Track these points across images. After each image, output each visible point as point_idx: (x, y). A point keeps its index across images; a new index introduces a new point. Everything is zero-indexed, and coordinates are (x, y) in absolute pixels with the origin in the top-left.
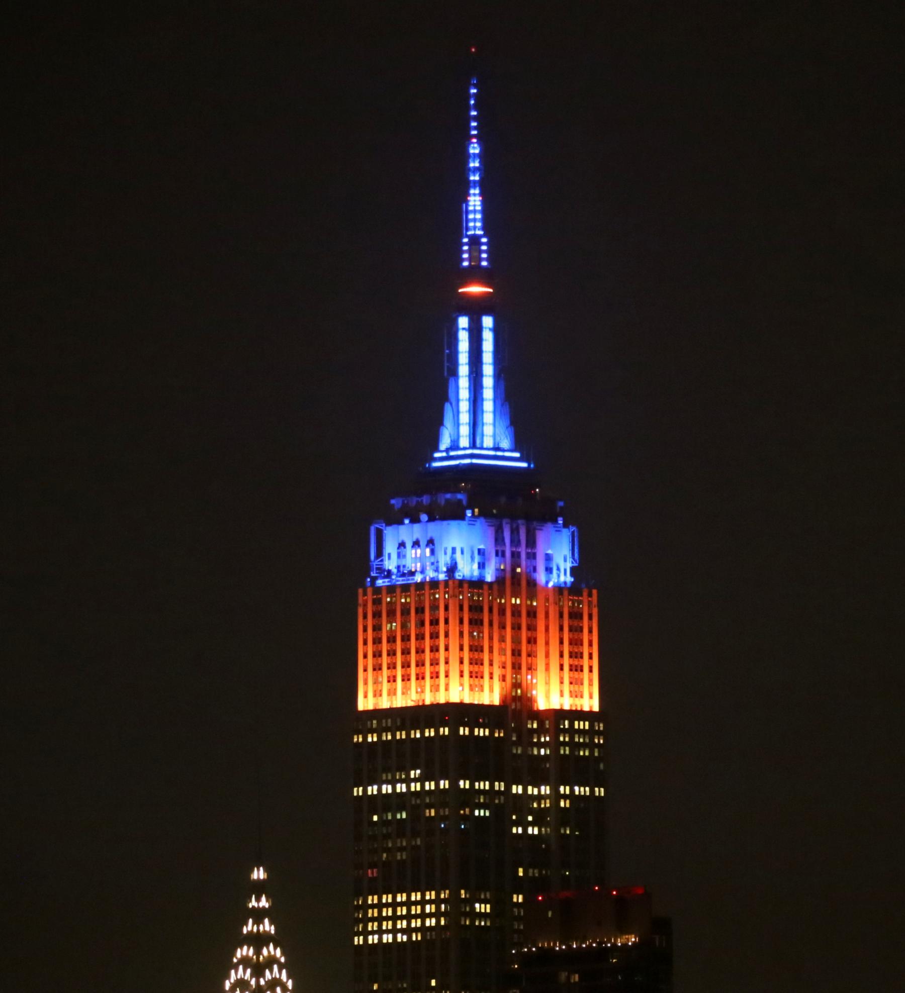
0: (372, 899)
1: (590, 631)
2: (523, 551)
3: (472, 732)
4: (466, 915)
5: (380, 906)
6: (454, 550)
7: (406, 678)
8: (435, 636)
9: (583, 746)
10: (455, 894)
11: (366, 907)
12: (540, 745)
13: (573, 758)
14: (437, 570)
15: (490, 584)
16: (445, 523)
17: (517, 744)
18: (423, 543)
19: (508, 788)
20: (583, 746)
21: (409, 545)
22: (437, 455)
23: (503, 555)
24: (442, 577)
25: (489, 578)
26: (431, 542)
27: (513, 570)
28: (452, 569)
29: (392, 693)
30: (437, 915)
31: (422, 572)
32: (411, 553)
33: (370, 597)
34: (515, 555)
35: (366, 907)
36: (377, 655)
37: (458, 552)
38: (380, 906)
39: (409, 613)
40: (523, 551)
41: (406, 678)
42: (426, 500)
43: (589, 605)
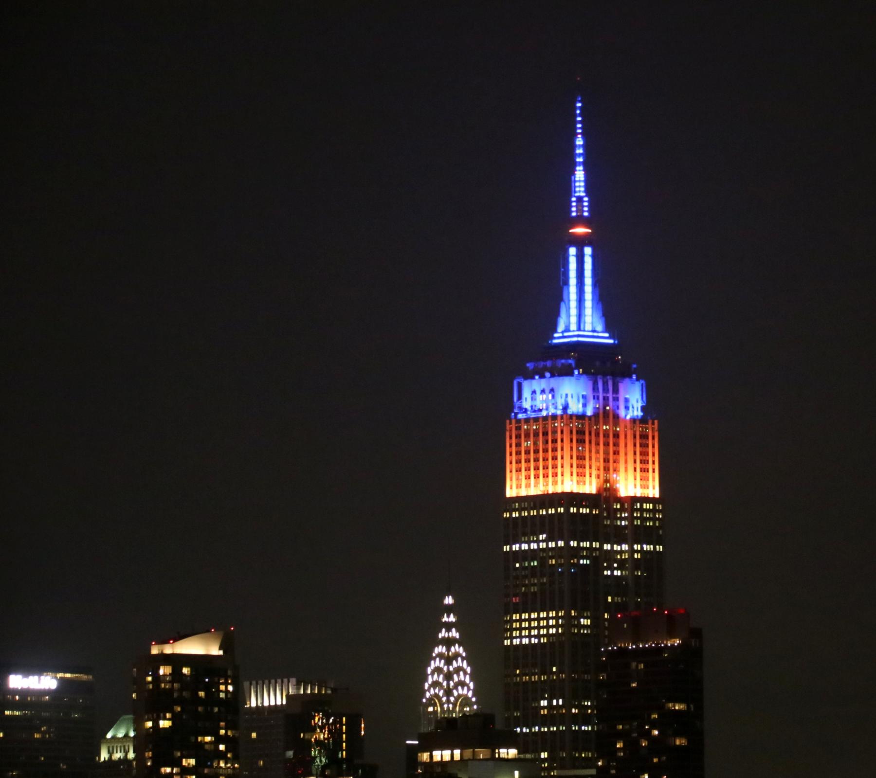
0: (516, 617)
1: (653, 447)
2: (610, 395)
3: (578, 510)
4: (575, 626)
5: (521, 621)
6: (567, 395)
7: (537, 477)
8: (555, 450)
9: (649, 519)
10: (568, 614)
11: (512, 621)
12: (622, 519)
13: (643, 527)
14: (556, 408)
15: (590, 418)
16: (561, 378)
17: (607, 518)
18: (547, 391)
19: (601, 546)
20: (649, 519)
21: (538, 392)
22: (556, 335)
23: (598, 398)
24: (559, 412)
25: (589, 413)
26: (552, 391)
27: (604, 408)
28: (565, 408)
29: (528, 486)
30: (557, 626)
31: (547, 409)
32: (540, 397)
33: (514, 425)
34: (606, 399)
35: (512, 621)
36: (518, 462)
37: (569, 396)
38: (521, 621)
39: (538, 435)
40: (610, 395)
41: (537, 477)
42: (549, 364)
43: (652, 430)
